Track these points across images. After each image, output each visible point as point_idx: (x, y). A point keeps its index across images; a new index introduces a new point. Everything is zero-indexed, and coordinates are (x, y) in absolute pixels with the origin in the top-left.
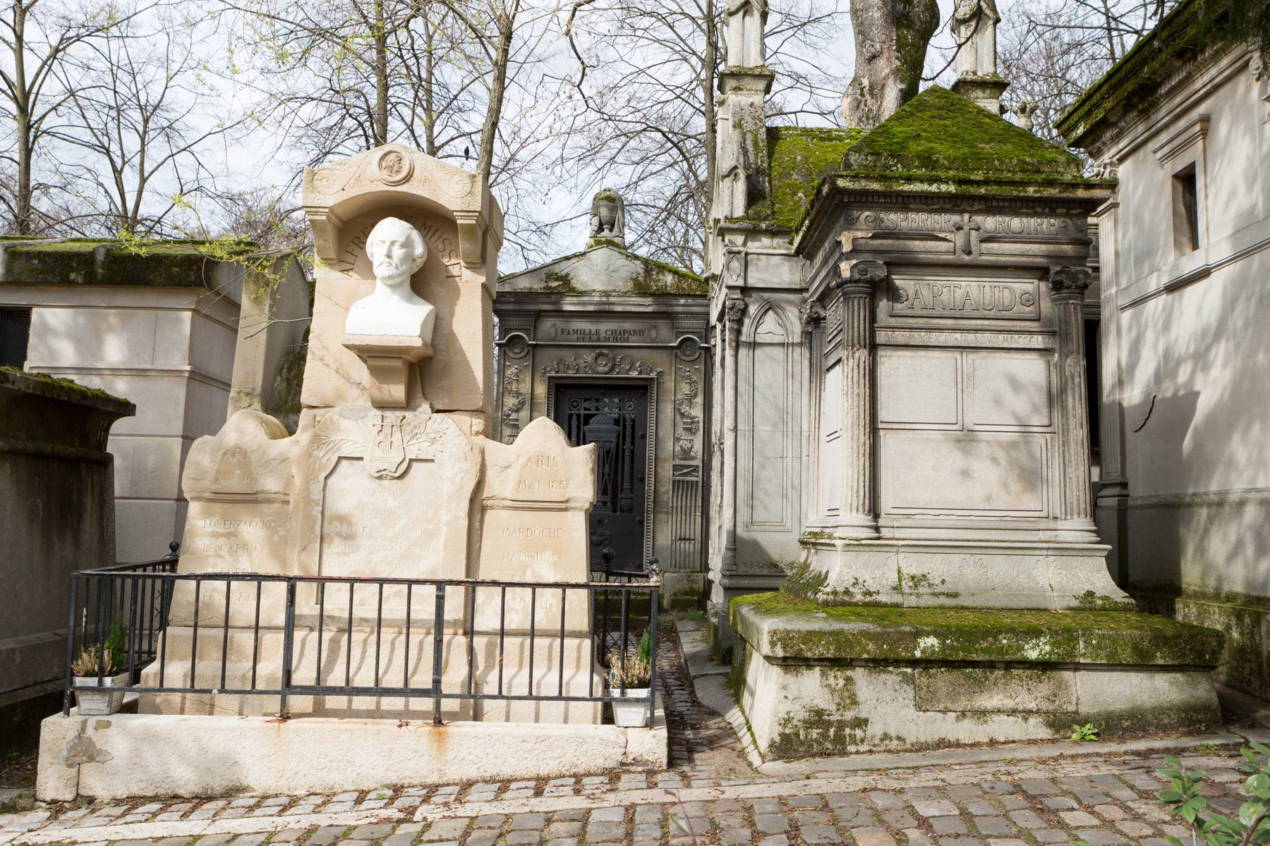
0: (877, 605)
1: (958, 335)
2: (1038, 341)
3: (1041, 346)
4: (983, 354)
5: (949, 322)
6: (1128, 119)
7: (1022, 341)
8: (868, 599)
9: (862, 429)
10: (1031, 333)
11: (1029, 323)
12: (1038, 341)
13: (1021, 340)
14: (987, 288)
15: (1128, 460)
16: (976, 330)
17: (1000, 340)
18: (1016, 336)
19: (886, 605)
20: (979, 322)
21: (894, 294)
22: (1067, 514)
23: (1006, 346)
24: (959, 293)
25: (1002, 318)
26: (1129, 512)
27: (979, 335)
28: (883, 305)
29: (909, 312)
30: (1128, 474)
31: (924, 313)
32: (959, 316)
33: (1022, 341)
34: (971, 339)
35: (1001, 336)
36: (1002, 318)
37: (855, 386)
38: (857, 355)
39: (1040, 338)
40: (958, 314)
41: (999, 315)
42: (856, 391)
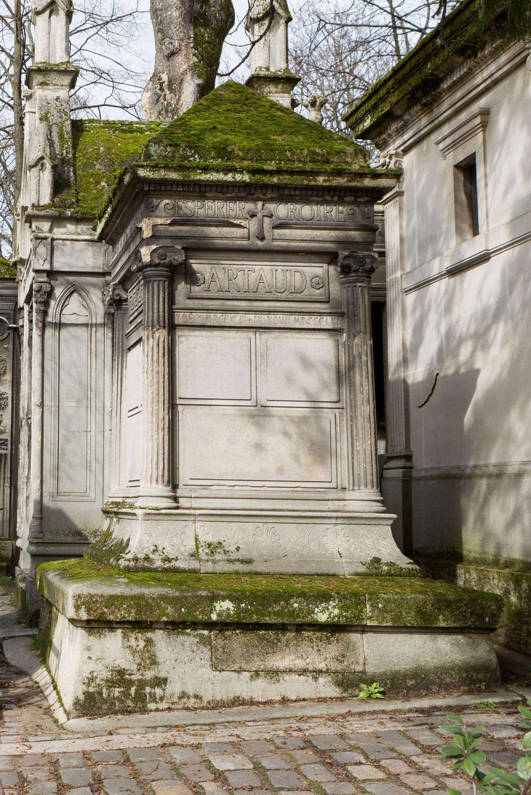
0: (176, 570)
1: (252, 316)
2: (327, 322)
3: (330, 327)
4: (276, 334)
5: (244, 304)
7: (312, 322)
8: (167, 565)
9: (161, 405)
10: (321, 314)
11: (319, 305)
12: (327, 322)
13: (311, 321)
14: (280, 272)
16: (269, 312)
17: (291, 321)
18: (307, 317)
19: (184, 571)
20: (272, 304)
21: (191, 277)
22: (355, 484)
23: (297, 326)
24: (253, 276)
25: (294, 300)
26: (414, 483)
27: (272, 316)
28: (182, 288)
29: (206, 295)
31: (220, 295)
32: (253, 298)
33: (312, 322)
34: (264, 320)
35: (292, 318)
36: (294, 300)
37: (155, 364)
39: (329, 319)
40: (251, 296)
41: (291, 297)
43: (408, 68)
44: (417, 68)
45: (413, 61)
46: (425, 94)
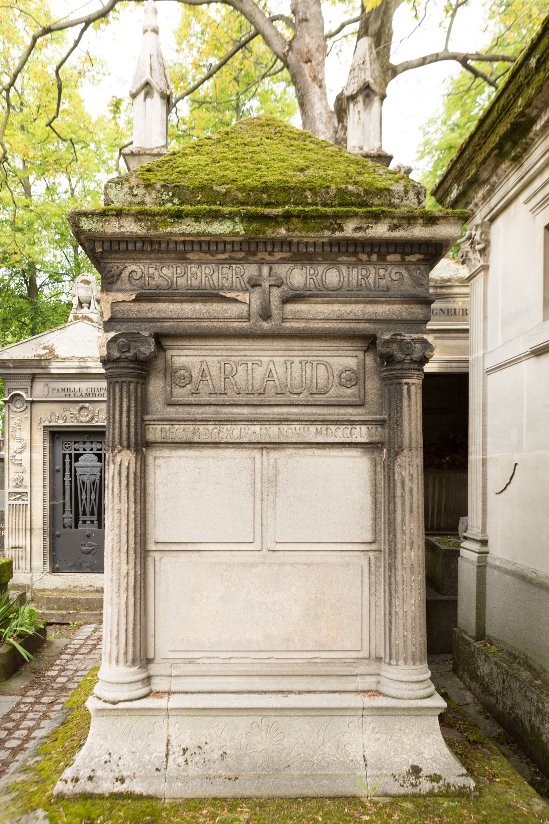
0: (130, 796)
1: (256, 428)
2: (361, 434)
3: (365, 440)
4: (290, 451)
5: (245, 410)
6: (499, 171)
7: (340, 434)
8: (119, 788)
9: (124, 556)
10: (353, 423)
11: (350, 410)
12: (361, 434)
13: (340, 433)
14: (296, 365)
15: (489, 519)
16: (280, 421)
17: (311, 433)
18: (333, 428)
19: (140, 797)
20: (285, 410)
21: (171, 374)
22: (390, 656)
23: (319, 439)
24: (259, 372)
25: (315, 404)
26: (488, 570)
27: (285, 427)
28: (156, 387)
29: (193, 399)
30: (489, 531)
31: (213, 399)
32: (258, 402)
33: (340, 434)
34: (273, 432)
35: (313, 428)
36: (315, 404)
37: (116, 500)
38: (118, 459)
39: (364, 428)
40: (256, 399)
41: (311, 399)
42: (117, 507)
43: (495, 113)
44: (506, 110)
45: (502, 101)
46: (515, 144)
